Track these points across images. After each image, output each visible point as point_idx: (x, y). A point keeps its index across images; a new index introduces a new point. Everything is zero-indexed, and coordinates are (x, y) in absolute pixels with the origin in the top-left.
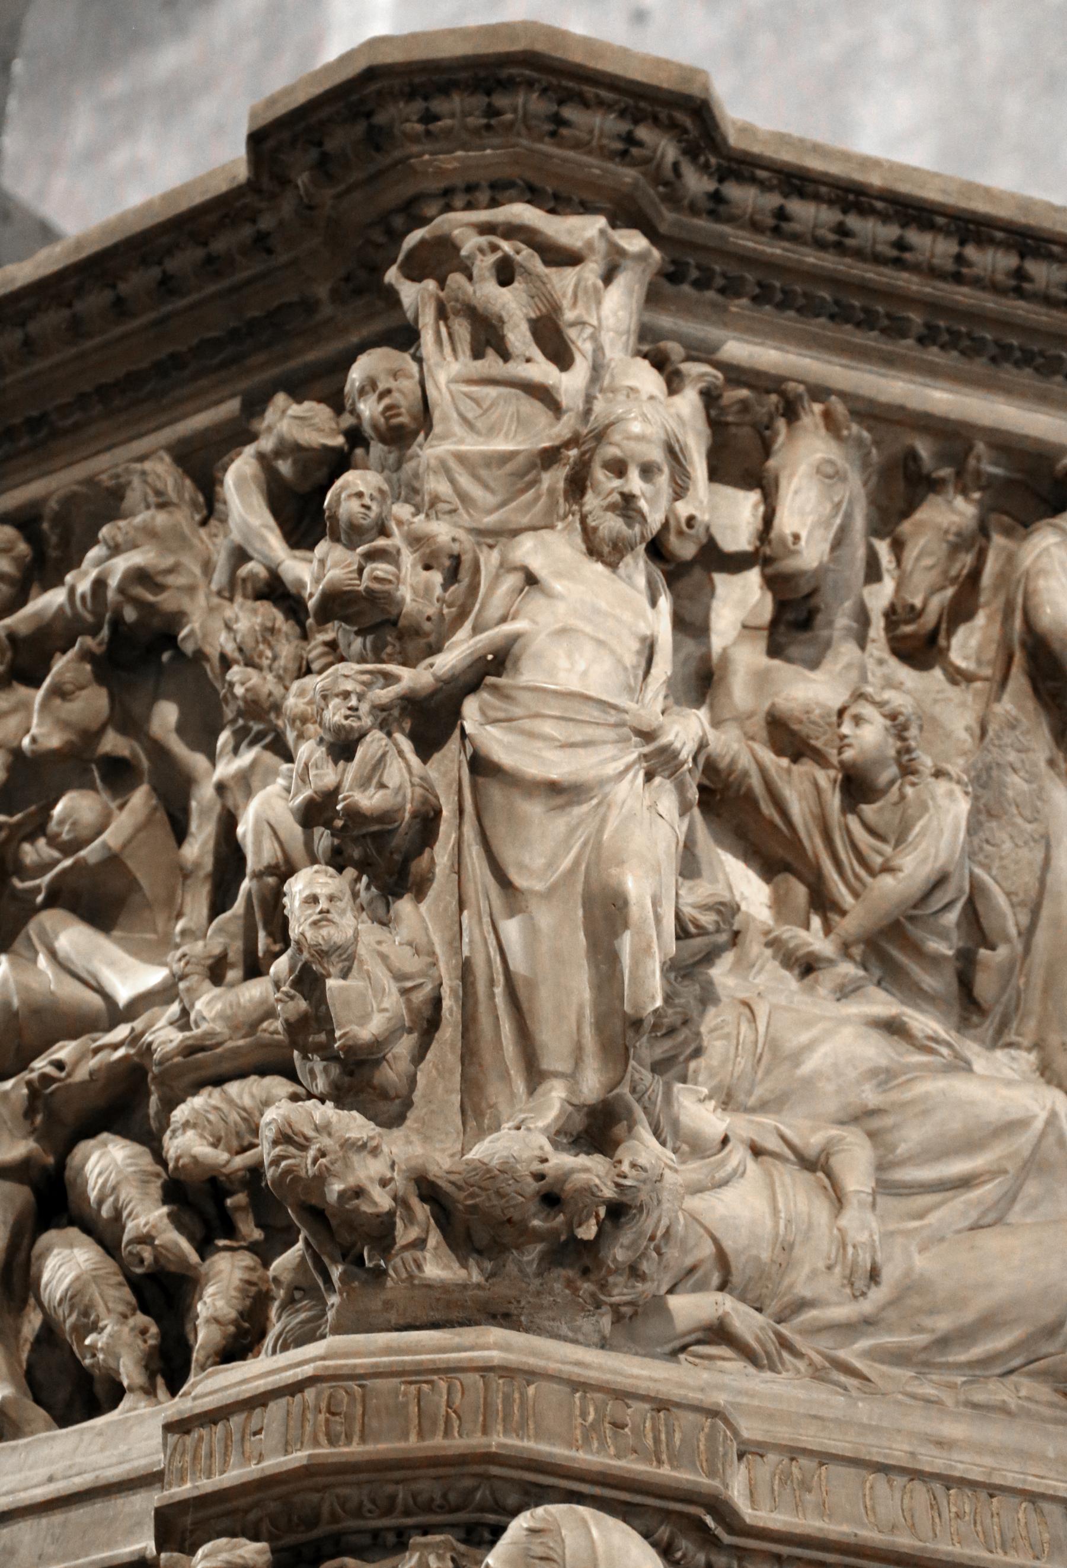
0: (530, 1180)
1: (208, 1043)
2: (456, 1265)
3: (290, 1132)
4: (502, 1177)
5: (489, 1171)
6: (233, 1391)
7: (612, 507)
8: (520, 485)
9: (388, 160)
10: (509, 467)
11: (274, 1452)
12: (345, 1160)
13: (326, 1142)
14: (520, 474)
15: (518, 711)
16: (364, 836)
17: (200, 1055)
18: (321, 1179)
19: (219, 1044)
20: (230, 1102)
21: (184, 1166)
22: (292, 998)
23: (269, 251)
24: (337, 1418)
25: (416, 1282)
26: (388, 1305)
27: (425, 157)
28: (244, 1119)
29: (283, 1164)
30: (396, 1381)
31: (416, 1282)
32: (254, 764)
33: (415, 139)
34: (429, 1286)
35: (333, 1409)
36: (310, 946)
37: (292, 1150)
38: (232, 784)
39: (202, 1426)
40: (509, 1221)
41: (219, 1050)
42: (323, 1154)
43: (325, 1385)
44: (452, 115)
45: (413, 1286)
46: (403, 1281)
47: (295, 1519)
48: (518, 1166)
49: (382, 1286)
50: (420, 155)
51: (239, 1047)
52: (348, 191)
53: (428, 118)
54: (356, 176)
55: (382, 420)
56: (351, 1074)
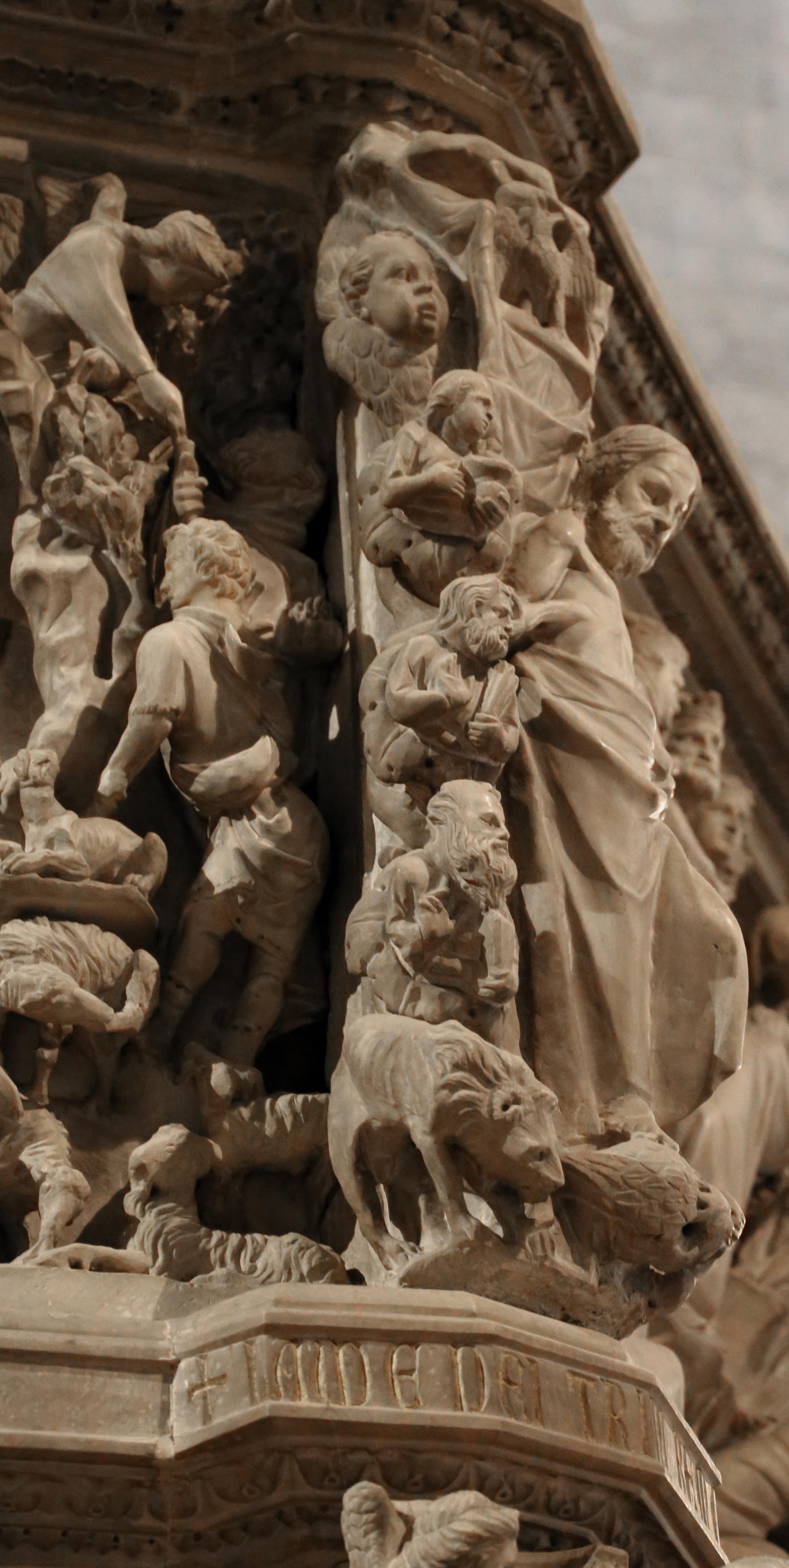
0: (694, 1204)
1: (71, 871)
2: (570, 1257)
3: (479, 1062)
4: (673, 1192)
5: (658, 1180)
6: (380, 1315)
7: (641, 529)
8: (545, 457)
9: (397, 35)
10: (543, 435)
11: (433, 1401)
12: (538, 1113)
13: (520, 1090)
14: (548, 446)
15: (601, 700)
16: (473, 763)
17: (58, 881)
18: (506, 1126)
19: (80, 878)
20: (81, 946)
21: (60, 1004)
22: (440, 910)
23: (170, 28)
24: (514, 1387)
25: (547, 1263)
26: (501, 1275)
27: (430, 55)
28: (93, 972)
29: (463, 1093)
30: (563, 1368)
31: (547, 1263)
32: (84, 572)
33: (432, 34)
34: (556, 1273)
35: (511, 1379)
36: (491, 869)
37: (475, 1081)
38: (50, 581)
39: (318, 1341)
40: (658, 1238)
41: (79, 884)
42: (517, 1100)
43: (501, 1348)
44: (477, 36)
45: (542, 1265)
46: (536, 1257)
47: (418, 1477)
48: (690, 1186)
49: (513, 1256)
50: (426, 52)
51: (100, 889)
52: (324, 35)
53: (454, 23)
54: (342, 28)
55: (415, 315)
56: (472, 1013)
